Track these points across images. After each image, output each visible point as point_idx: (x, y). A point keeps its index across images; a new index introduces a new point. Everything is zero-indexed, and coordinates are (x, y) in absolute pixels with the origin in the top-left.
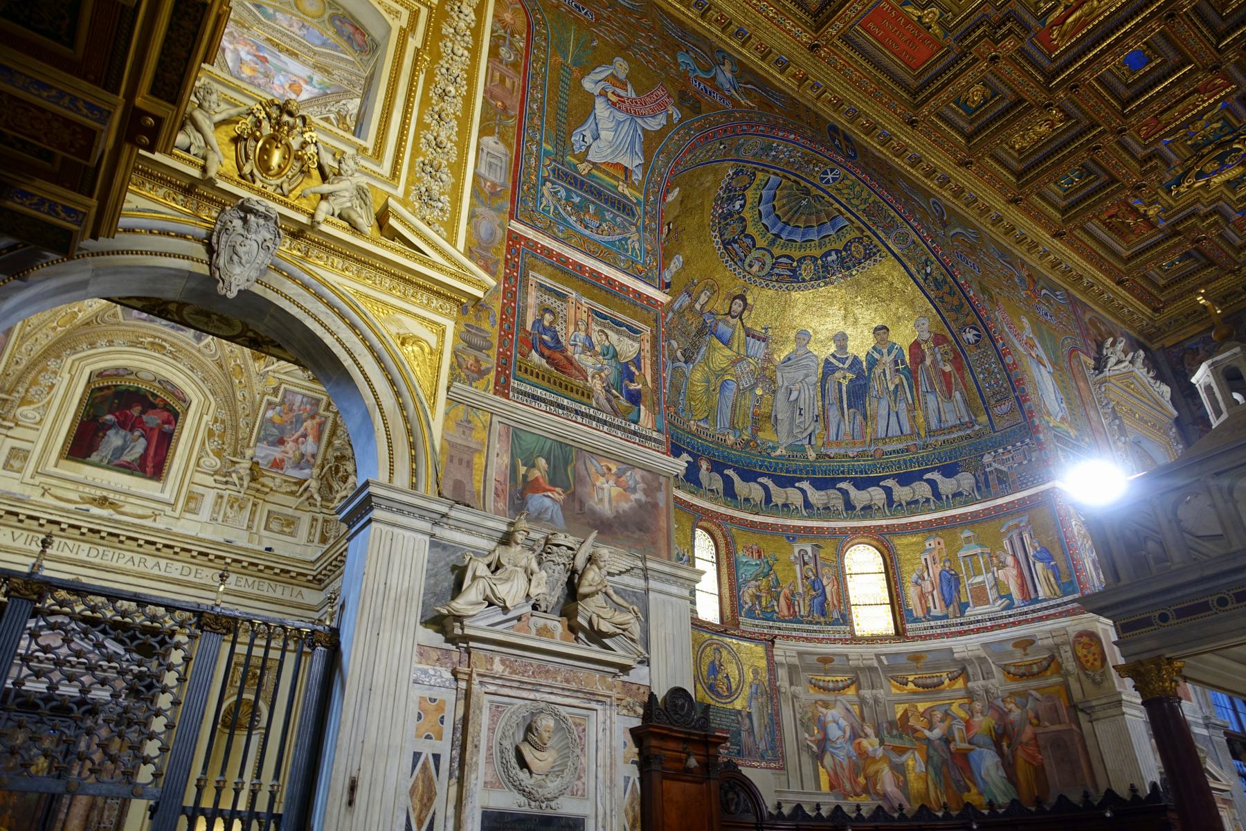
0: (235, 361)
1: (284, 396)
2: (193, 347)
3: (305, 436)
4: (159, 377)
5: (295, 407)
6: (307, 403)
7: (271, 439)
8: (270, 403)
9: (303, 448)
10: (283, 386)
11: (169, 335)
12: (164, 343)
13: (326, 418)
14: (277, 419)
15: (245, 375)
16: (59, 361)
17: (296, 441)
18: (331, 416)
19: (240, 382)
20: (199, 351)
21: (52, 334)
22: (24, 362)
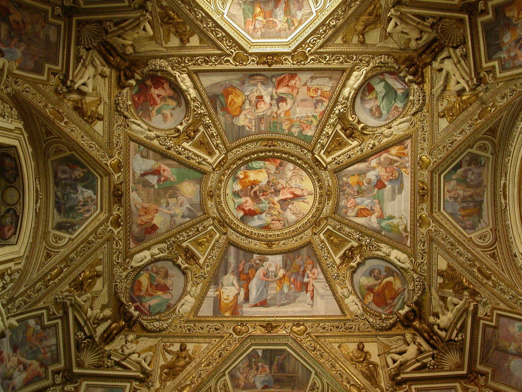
0: (65, 267)
1: (49, 327)
2: (46, 226)
3: (25, 368)
4: (18, 208)
5: (45, 343)
6: (51, 351)
7: (14, 337)
8: (40, 317)
9: (16, 373)
10: (59, 321)
11: (47, 203)
12: (39, 200)
13: (47, 378)
14: (30, 331)
15: (56, 280)
16: (16, 117)
17: (20, 363)
18: (50, 382)
19: (49, 280)
20: (46, 233)
21: (41, 105)
22: (19, 88)
